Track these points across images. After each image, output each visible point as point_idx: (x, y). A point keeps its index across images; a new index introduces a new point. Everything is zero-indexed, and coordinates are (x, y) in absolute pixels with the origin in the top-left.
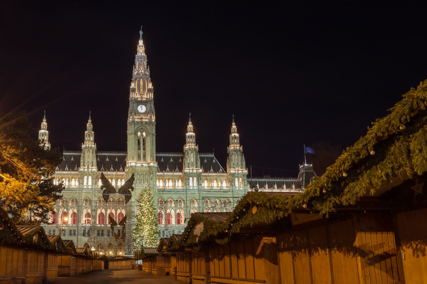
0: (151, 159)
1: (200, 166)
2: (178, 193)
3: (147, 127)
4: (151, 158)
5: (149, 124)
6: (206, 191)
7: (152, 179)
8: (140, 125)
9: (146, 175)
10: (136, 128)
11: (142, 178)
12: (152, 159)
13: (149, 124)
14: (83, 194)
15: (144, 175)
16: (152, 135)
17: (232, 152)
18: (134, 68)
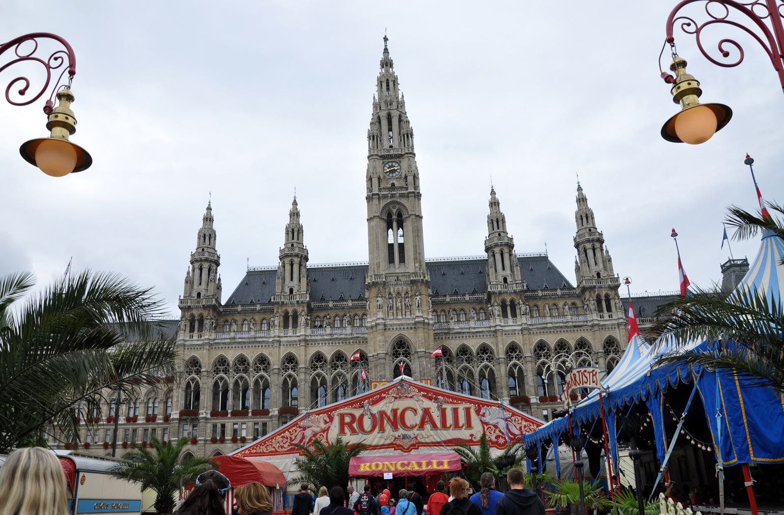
0: (415, 265)
1: (520, 277)
2: (478, 334)
3: (403, 203)
4: (415, 263)
5: (408, 197)
6: (537, 328)
7: (419, 306)
8: (389, 201)
9: (407, 299)
10: (382, 206)
11: (399, 305)
12: (417, 265)
13: (408, 197)
14: (282, 346)
15: (403, 300)
16: (414, 217)
17: (583, 245)
18: (377, 98)
